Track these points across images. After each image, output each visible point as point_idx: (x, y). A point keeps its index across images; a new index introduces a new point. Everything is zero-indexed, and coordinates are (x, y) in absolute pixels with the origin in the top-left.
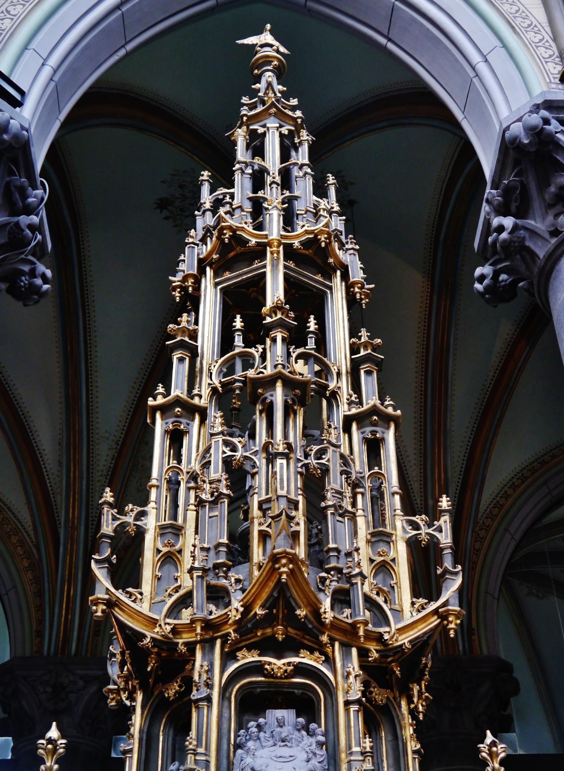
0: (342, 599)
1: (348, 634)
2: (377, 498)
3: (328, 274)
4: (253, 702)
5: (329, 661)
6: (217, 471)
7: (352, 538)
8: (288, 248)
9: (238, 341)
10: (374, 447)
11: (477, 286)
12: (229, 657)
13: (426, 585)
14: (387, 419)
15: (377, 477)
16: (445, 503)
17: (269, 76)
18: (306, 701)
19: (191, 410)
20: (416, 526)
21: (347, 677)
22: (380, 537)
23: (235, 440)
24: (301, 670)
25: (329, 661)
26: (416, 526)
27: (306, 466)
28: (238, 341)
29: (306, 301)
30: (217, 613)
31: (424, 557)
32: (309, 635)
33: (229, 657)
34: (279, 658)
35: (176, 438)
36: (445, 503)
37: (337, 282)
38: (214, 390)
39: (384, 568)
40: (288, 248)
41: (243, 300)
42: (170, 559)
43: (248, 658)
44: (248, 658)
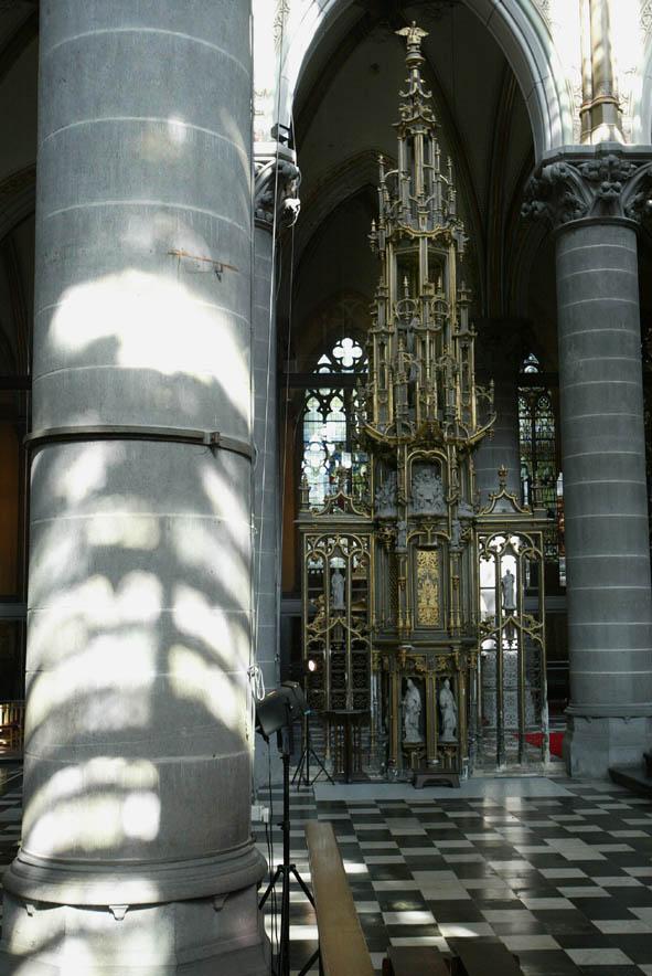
0: (452, 428)
1: (453, 442)
2: (465, 374)
3: (448, 246)
4: (420, 463)
5: (446, 452)
6: (401, 371)
7: (456, 401)
8: (429, 239)
9: (407, 291)
10: (465, 349)
11: (523, 213)
12: (410, 450)
13: (482, 420)
14: (471, 337)
15: (466, 367)
16: (492, 384)
17: (416, 73)
18: (435, 465)
19: (388, 334)
20: (480, 391)
21: (450, 455)
22: (466, 396)
23: (409, 355)
24: (435, 454)
25: (446, 452)
26: (480, 391)
27: (438, 368)
28: (407, 291)
29: (437, 266)
30: (406, 436)
31: (482, 405)
32: (440, 445)
33: (410, 450)
34: (427, 450)
35: (382, 346)
36: (492, 384)
37: (452, 251)
38: (396, 318)
39: (467, 409)
40: (429, 239)
41: (408, 266)
42: (384, 406)
43: (416, 451)
44: (416, 451)
